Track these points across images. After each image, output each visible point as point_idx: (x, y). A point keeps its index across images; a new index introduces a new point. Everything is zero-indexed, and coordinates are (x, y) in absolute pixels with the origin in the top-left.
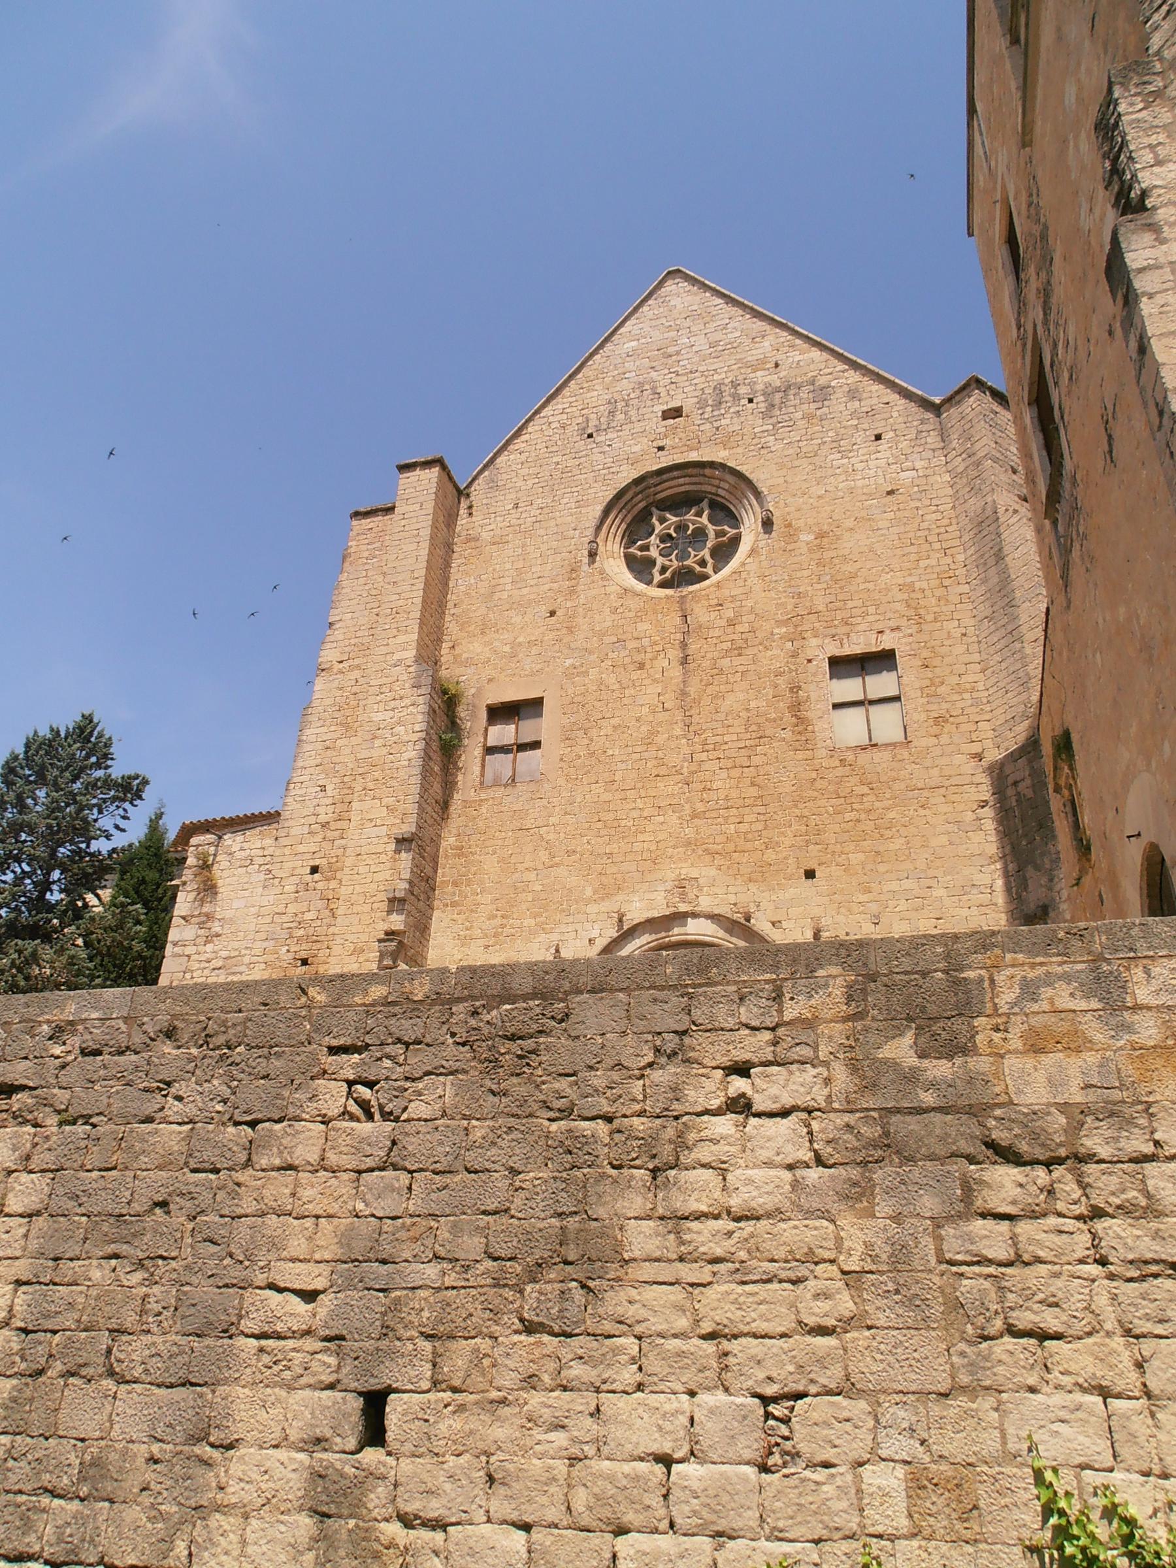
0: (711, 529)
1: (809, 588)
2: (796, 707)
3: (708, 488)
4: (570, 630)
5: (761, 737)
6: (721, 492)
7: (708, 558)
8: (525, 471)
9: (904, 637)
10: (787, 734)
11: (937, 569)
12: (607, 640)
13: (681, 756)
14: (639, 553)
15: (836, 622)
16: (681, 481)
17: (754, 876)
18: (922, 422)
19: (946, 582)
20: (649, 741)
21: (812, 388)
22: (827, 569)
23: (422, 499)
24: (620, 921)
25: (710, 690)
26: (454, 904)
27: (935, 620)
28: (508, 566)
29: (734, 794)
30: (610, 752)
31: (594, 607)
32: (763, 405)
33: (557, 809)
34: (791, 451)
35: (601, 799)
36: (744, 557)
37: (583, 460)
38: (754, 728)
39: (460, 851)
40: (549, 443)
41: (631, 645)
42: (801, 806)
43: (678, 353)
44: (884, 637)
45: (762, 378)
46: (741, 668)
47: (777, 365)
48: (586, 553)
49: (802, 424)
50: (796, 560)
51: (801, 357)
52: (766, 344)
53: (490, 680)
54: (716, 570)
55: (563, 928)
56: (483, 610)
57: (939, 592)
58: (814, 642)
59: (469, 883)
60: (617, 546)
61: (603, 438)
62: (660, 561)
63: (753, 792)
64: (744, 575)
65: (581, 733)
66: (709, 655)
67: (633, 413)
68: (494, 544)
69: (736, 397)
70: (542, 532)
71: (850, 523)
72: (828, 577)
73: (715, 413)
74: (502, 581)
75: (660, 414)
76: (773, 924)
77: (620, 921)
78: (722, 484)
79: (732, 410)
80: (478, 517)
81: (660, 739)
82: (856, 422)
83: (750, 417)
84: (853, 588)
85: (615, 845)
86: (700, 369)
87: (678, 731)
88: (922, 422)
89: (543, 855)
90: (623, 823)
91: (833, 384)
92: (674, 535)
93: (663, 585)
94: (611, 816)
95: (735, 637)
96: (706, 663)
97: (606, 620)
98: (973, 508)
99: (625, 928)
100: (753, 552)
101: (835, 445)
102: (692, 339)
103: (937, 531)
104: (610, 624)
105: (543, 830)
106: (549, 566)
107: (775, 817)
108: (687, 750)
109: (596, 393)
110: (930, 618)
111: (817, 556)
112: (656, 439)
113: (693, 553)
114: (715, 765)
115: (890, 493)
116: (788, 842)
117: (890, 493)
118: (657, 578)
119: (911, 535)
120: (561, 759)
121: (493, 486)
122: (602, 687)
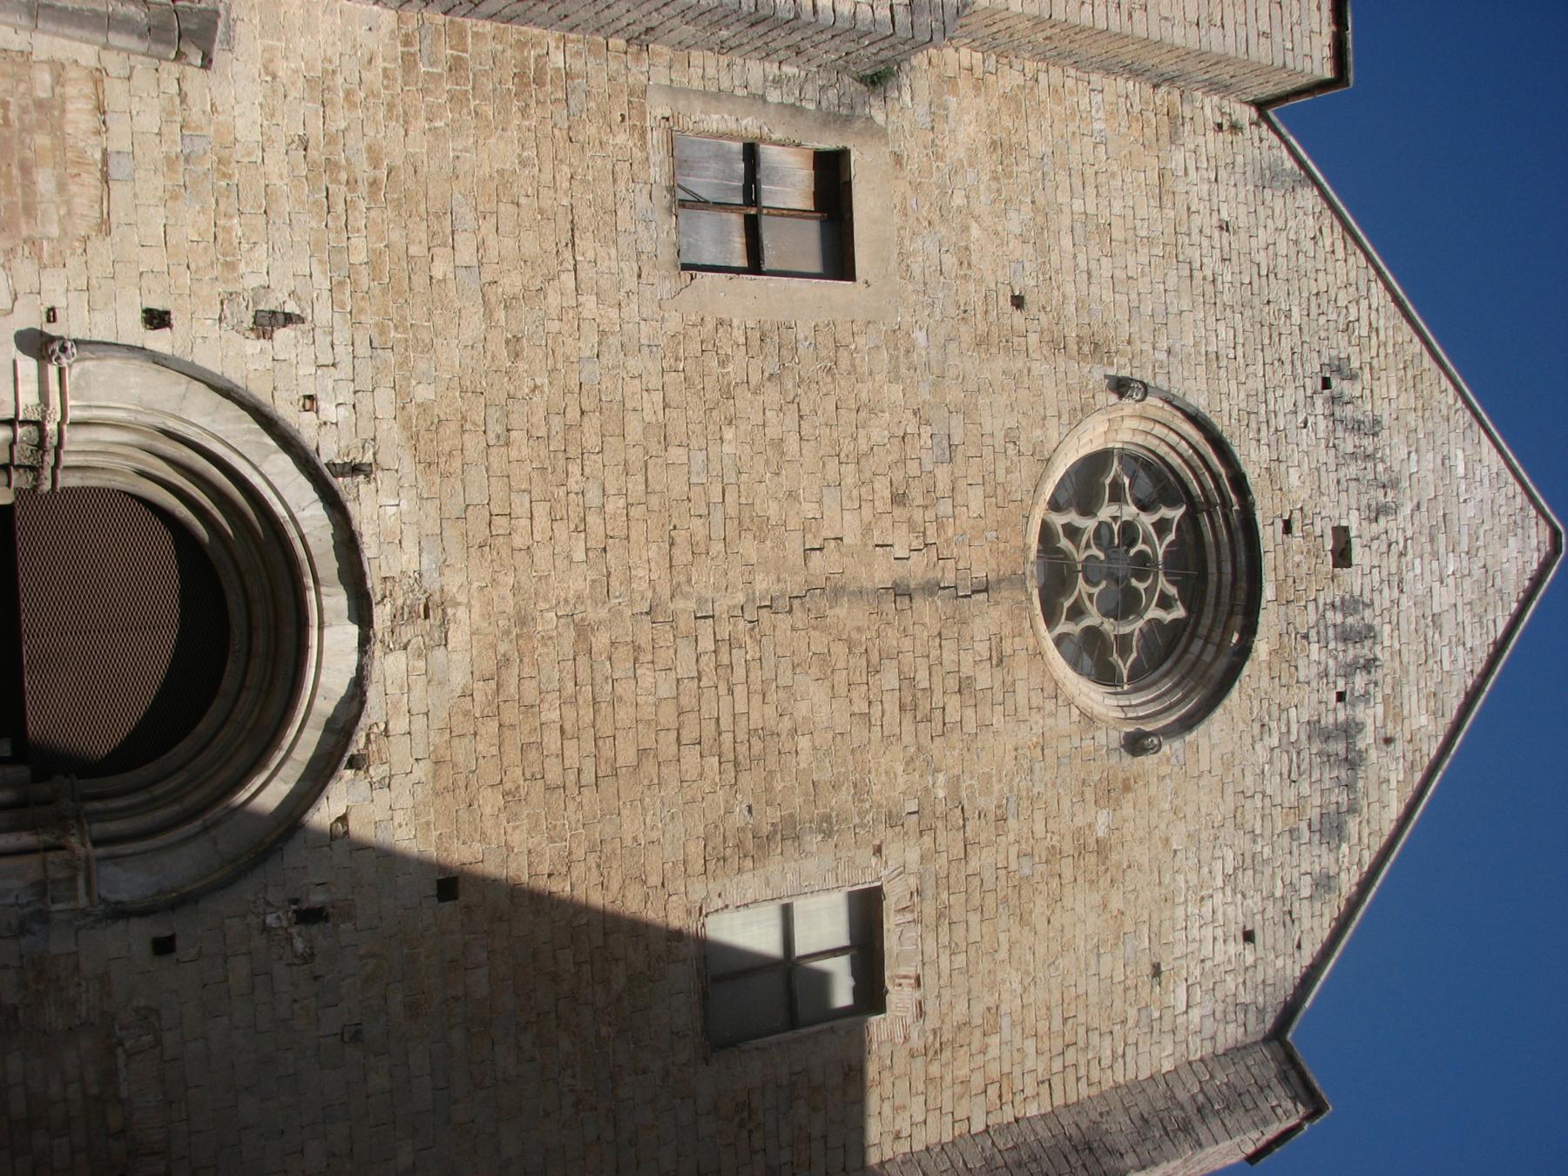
0: (1134, 627)
1: (1011, 837)
2: (788, 833)
3: (1206, 621)
4: (982, 342)
5: (736, 763)
6: (1197, 645)
7: (1086, 622)
8: (1282, 248)
9: (905, 1027)
10: (739, 817)
11: (1017, 1070)
12: (957, 421)
13: (709, 595)
14: (1108, 481)
15: (944, 896)
16: (1227, 568)
17: (446, 771)
18: (1261, 1012)
19: (993, 1091)
20: (750, 523)
21: (1344, 809)
22: (1042, 868)
23: (1277, 37)
24: (355, 469)
25: (840, 649)
26: (409, 62)
27: (929, 1080)
28: (1117, 207)
29: (624, 714)
30: (729, 434)
31: (1023, 393)
32: (1331, 719)
33: (613, 313)
34: (1249, 779)
35: (630, 416)
36: (1082, 701)
37: (1288, 366)
38: (757, 746)
39: (530, 79)
40: (1324, 298)
41: (943, 475)
42: (592, 859)
43: (1435, 555)
44: (907, 990)
45: (1371, 716)
46: (876, 711)
47: (1388, 741)
48: (1125, 373)
49: (1290, 795)
50: (1066, 804)
51: (1393, 784)
52: (1424, 720)
53: (898, 159)
54: (1058, 641)
56: (1039, 147)
57: (977, 1081)
58: (913, 856)
59: (456, 99)
60: (1127, 437)
61: (1319, 409)
62: (1089, 524)
63: (627, 755)
64: (1050, 706)
65: (772, 366)
66: (907, 644)
67: (1353, 470)
68: (1161, 176)
69: (1349, 670)
70: (1172, 281)
71: (1116, 903)
72: (1027, 871)
73: (1331, 632)
74: (1090, 190)
75: (1344, 523)
77: (355, 469)
78: (1211, 649)
79: (1331, 663)
80: (1214, 143)
81: (748, 548)
82: (1278, 893)
83: (1315, 697)
84: (1003, 921)
85: (525, 452)
86: (1404, 598)
87: (763, 583)
88: (1261, 1012)
89: (512, 282)
90: (574, 469)
91: (1344, 847)
92: (1132, 552)
93: (1046, 531)
94: (592, 441)
95: (938, 699)
96: (892, 638)
97: (995, 422)
98: (1115, 1128)
99: (339, 483)
100: (1089, 719)
101: (1248, 861)
102: (1451, 581)
103: (1082, 1061)
104: (987, 429)
105: (568, 280)
106: (1107, 296)
107: (572, 806)
108: (721, 607)
109: (1393, 394)
110: (935, 1069)
111: (1068, 847)
112: (1304, 517)
113: (1096, 591)
114: (686, 667)
115: (1157, 971)
116: (518, 838)
117: (1157, 971)
118: (1059, 520)
119: (1081, 1018)
120: (721, 323)
121: (1268, 179)
122: (863, 414)
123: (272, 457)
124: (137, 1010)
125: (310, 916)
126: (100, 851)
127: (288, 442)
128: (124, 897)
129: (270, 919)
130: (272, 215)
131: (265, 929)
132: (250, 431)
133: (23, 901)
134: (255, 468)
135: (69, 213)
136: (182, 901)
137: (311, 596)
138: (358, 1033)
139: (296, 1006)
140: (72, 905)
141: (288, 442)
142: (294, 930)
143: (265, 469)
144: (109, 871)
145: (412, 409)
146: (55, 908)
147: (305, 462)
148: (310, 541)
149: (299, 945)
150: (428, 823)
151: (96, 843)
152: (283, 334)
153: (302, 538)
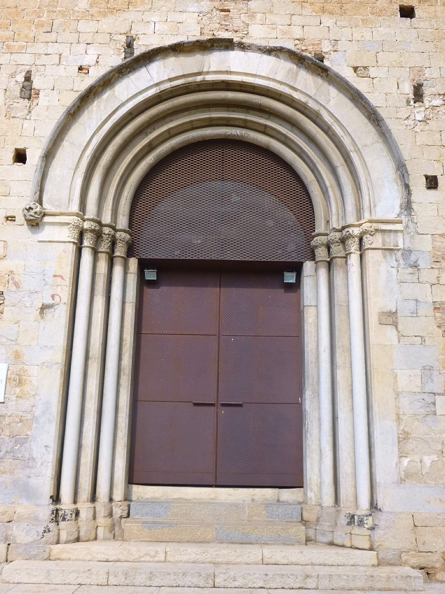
17: (329, 7)
24: (129, 45)
55: (40, 48)
76: (355, 69)
77: (129, 45)
99: (137, 52)
123: (116, 94)
125: (418, 94)
127: (107, 82)
129: (419, 117)
131: (425, 121)
133: (395, 264)
134: (123, 104)
136: (401, 168)
137: (209, 78)
141: (107, 82)
142: (427, 104)
143: (124, 99)
145: (94, 11)
148: (173, 75)
150: (363, 20)
152: (36, 84)
153: (170, 80)
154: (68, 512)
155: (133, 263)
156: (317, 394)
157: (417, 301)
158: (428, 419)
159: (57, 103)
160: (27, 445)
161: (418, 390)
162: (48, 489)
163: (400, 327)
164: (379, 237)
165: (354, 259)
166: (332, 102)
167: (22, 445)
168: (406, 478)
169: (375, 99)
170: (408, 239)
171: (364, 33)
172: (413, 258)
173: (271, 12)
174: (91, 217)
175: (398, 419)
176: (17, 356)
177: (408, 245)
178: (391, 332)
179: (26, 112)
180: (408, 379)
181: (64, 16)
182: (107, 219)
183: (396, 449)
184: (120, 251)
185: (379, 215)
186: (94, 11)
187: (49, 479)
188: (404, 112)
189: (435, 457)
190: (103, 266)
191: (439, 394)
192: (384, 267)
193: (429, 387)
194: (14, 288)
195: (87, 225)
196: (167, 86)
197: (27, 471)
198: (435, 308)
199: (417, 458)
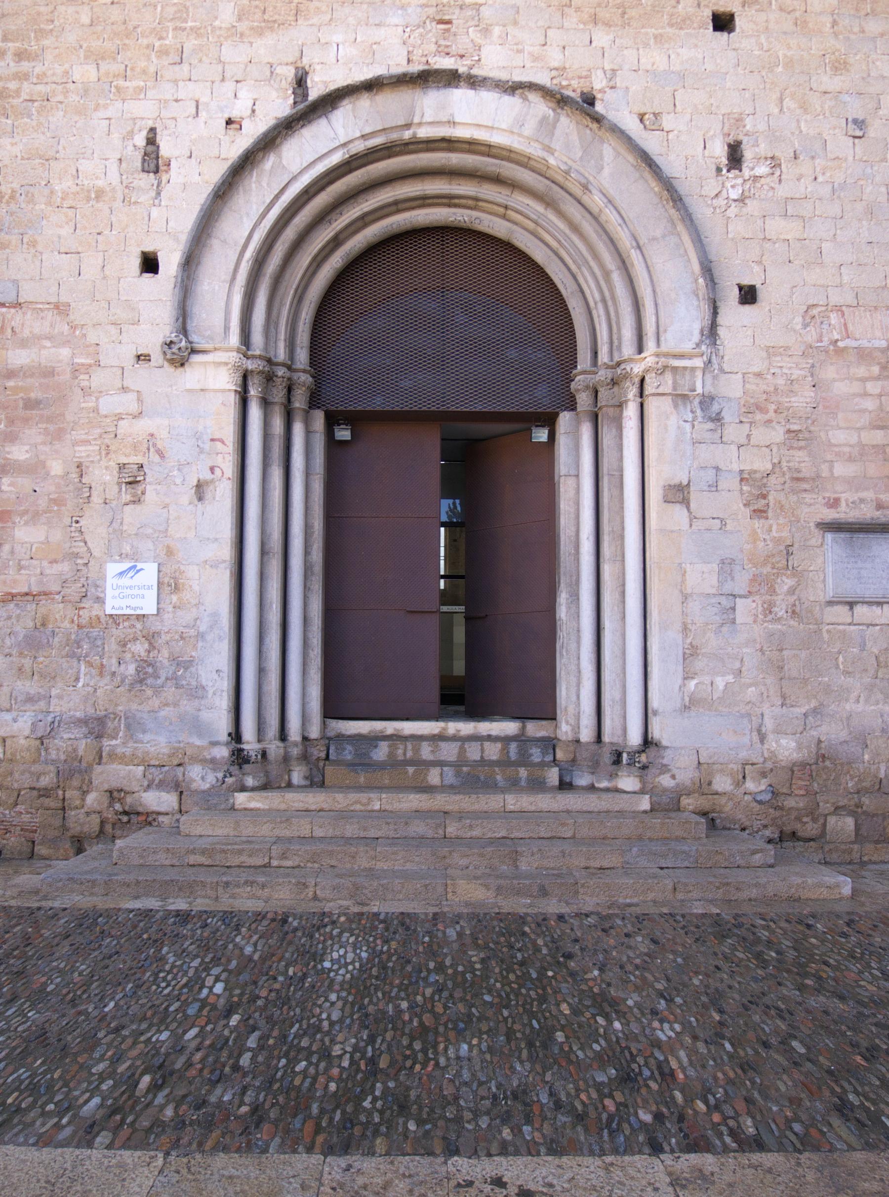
17: (603, 14)
24: (301, 82)
55: (167, 91)
77: (301, 82)
123: (284, 162)
124: (805, 326)
126: (650, 345)
128: (696, 327)
129: (734, 194)
130: (51, 153)
131: (742, 200)
132: (259, 182)
133: (690, 417)
135: (49, 338)
137: (423, 133)
138: (855, 121)
139: (820, 179)
140: (699, 374)
141: (269, 142)
142: (746, 173)
144: (670, 343)
145: (243, 26)
146: (699, 390)
147: (287, 126)
148: (368, 130)
149: (762, 169)
150: (655, 37)
151: (640, 350)
152: (166, 148)
154: (253, 754)
155: (319, 419)
156: (575, 596)
157: (717, 469)
158: (725, 629)
159: (197, 178)
160: (193, 669)
161: (713, 591)
162: (222, 725)
163: (693, 505)
164: (668, 377)
165: (631, 411)
166: (606, 171)
167: (186, 669)
168: (690, 705)
169: (672, 165)
170: (709, 381)
171: (654, 58)
172: (715, 407)
173: (515, 23)
174: (258, 353)
175: (685, 629)
176: (170, 552)
177: (709, 388)
178: (679, 513)
179: (153, 194)
180: (702, 577)
181: (199, 36)
182: (281, 354)
183: (680, 668)
184: (299, 402)
185: (670, 343)
186: (243, 26)
187: (225, 712)
188: (711, 186)
189: (730, 678)
190: (278, 424)
191: (741, 596)
192: (673, 421)
193: (728, 587)
194: (156, 458)
195: (250, 365)
196: (359, 147)
197: (196, 703)
198: (742, 480)
199: (707, 679)
